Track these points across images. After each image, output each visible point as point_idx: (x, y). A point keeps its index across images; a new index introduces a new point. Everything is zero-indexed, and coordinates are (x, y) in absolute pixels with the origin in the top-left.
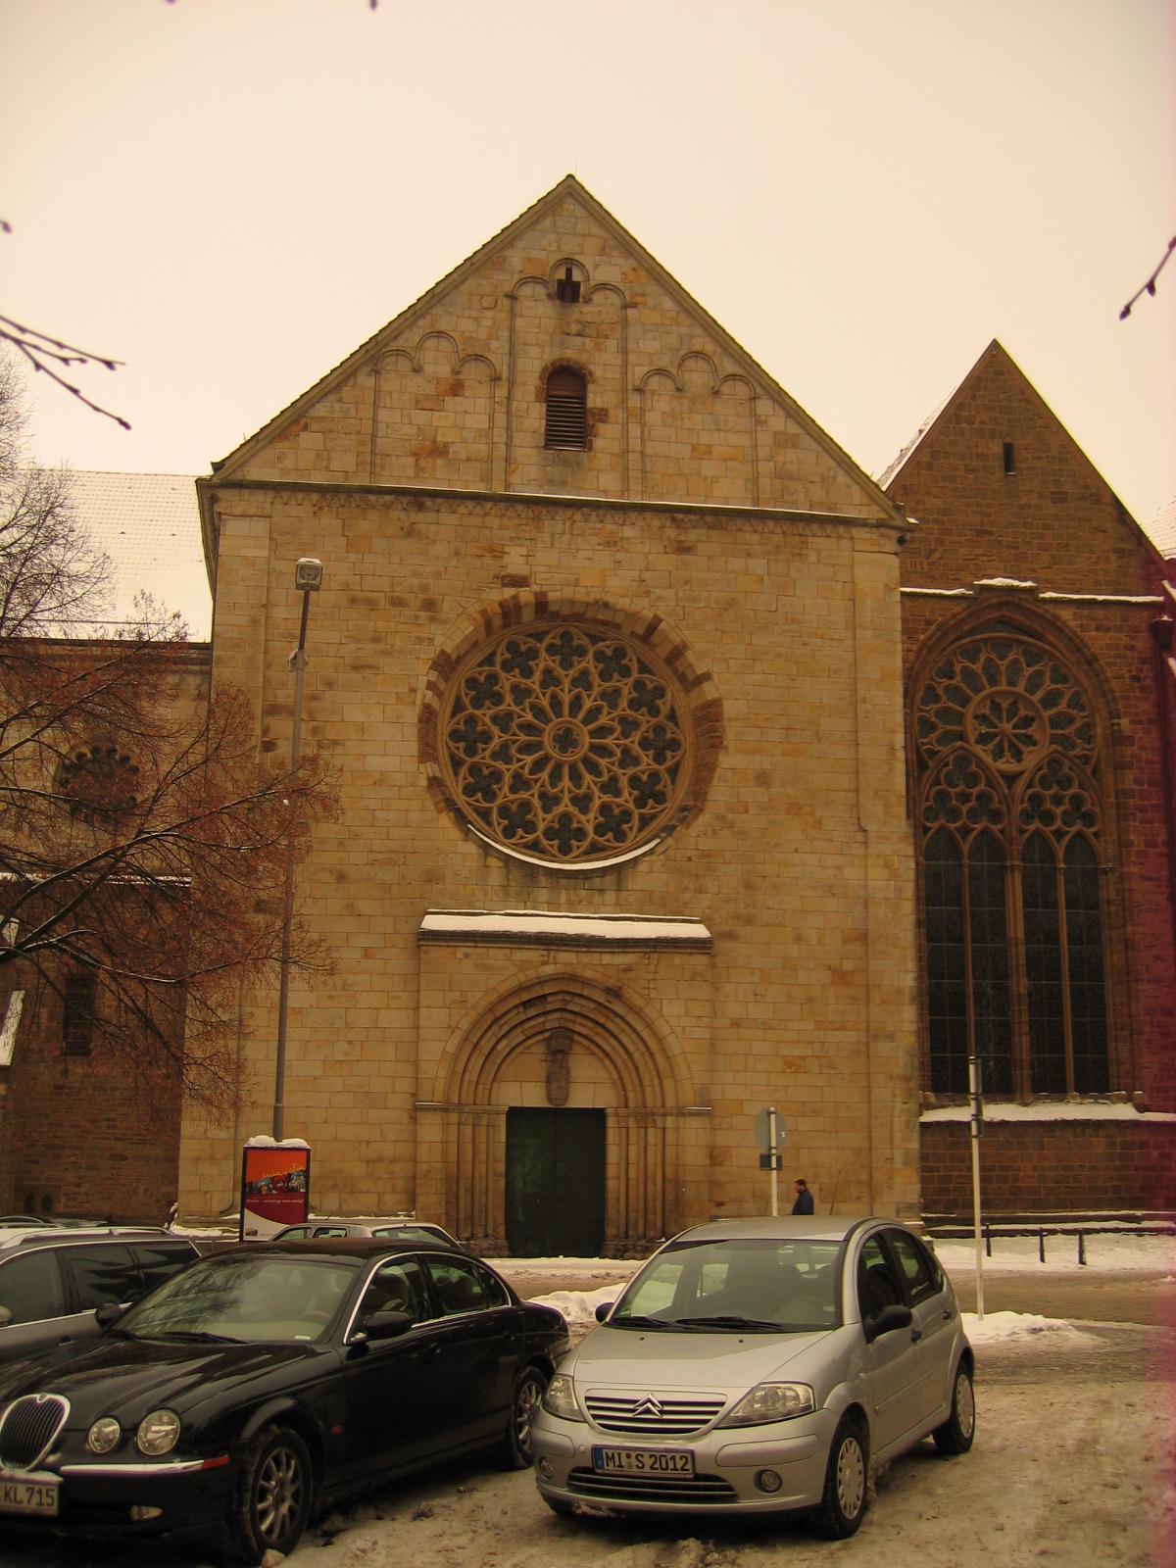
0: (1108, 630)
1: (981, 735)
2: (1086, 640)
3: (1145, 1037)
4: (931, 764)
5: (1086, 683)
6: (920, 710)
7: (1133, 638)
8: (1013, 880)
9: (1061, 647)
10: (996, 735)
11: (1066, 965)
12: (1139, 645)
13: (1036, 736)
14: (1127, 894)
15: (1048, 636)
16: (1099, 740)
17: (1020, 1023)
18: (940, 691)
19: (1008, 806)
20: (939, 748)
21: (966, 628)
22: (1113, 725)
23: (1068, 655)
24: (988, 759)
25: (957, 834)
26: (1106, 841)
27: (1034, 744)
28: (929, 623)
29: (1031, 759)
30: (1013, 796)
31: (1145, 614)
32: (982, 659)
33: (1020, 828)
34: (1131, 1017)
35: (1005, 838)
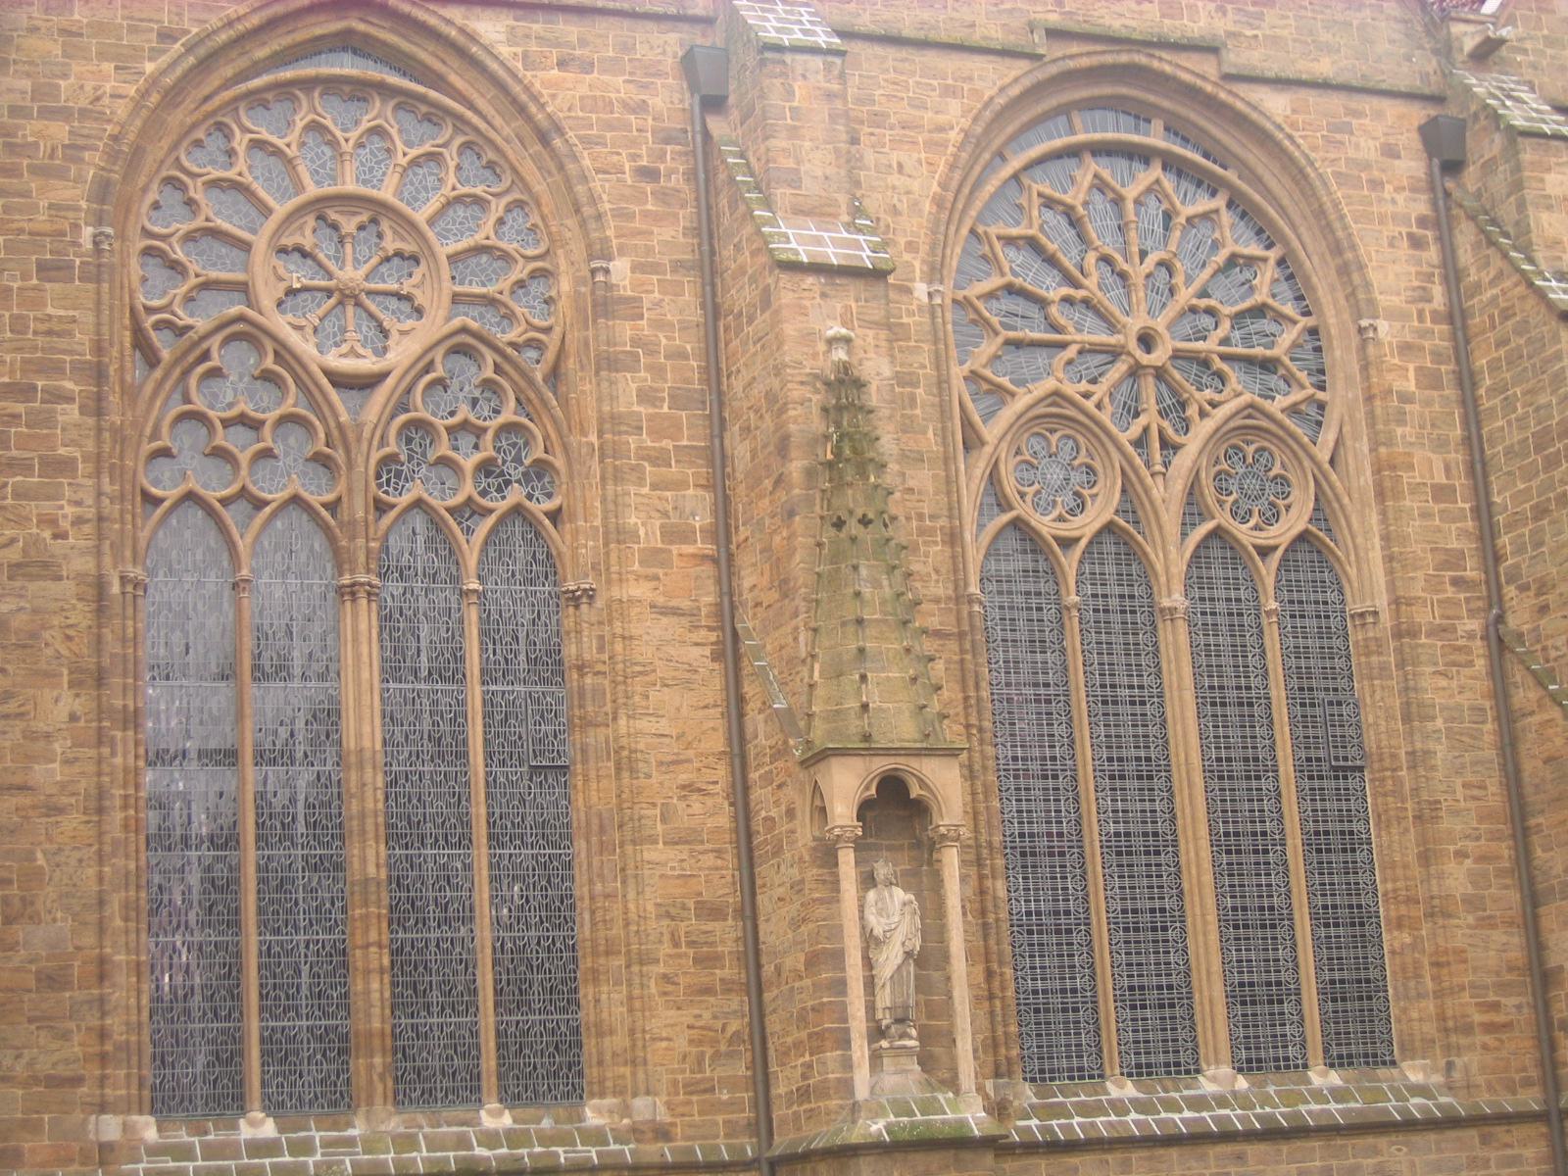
0: (587, 67)
1: (291, 292)
2: (537, 85)
3: (661, 969)
4: (166, 354)
5: (539, 187)
6: (147, 233)
7: (644, 87)
8: (355, 616)
9: (481, 103)
10: (329, 293)
11: (479, 811)
12: (657, 102)
13: (420, 299)
14: (619, 647)
15: (453, 78)
16: (564, 304)
17: (367, 946)
18: (197, 192)
19: (348, 451)
20: (190, 321)
21: (261, 53)
22: (593, 272)
23: (498, 121)
24: (305, 346)
25: (227, 515)
26: (576, 533)
27: (419, 312)
28: (167, 36)
29: (401, 353)
30: (360, 426)
31: (673, 38)
32: (300, 125)
33: (377, 502)
34: (627, 924)
35: (341, 525)
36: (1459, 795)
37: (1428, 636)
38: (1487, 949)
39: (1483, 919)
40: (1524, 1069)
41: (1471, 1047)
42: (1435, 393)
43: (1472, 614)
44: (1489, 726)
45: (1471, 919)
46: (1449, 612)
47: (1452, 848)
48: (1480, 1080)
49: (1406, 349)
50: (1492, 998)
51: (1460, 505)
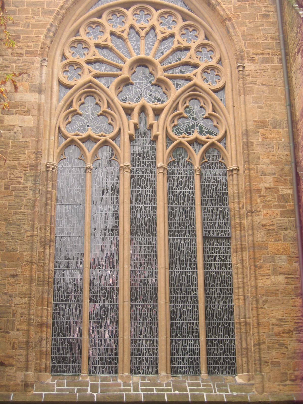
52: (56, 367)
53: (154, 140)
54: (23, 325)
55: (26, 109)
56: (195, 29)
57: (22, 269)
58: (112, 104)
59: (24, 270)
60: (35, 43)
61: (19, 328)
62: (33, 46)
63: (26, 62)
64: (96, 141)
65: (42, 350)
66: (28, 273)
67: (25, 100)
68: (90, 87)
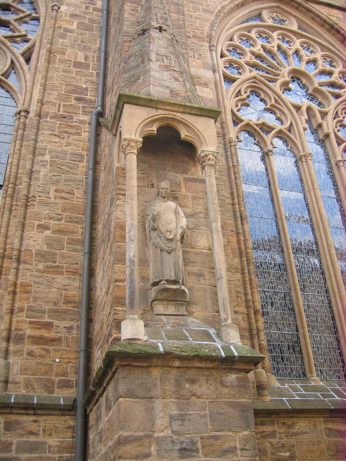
36: (52, 194)
37: (52, 118)
38: (49, 287)
39: (52, 267)
40: (65, 374)
41: (16, 353)
42: (88, 32)
43: (85, 113)
44: (84, 164)
45: (41, 266)
46: (70, 111)
47: (37, 223)
48: (21, 378)
49: (74, 16)
50: (47, 319)
51: (91, 71)
52: (275, 370)
53: (323, 139)
54: (242, 306)
55: (203, 82)
56: (332, 60)
57: (228, 239)
58: (279, 101)
59: (231, 241)
60: (201, 31)
61: (237, 311)
62: (199, 33)
63: (195, 44)
64: (269, 130)
65: (263, 344)
66: (236, 245)
67: (201, 74)
68: (254, 82)
